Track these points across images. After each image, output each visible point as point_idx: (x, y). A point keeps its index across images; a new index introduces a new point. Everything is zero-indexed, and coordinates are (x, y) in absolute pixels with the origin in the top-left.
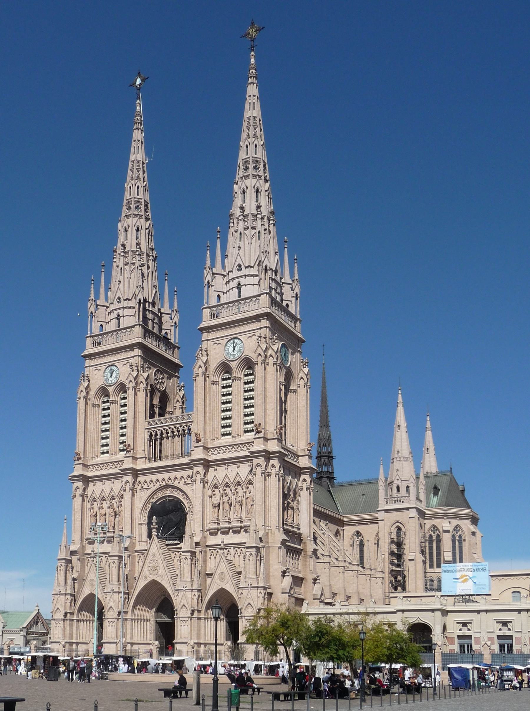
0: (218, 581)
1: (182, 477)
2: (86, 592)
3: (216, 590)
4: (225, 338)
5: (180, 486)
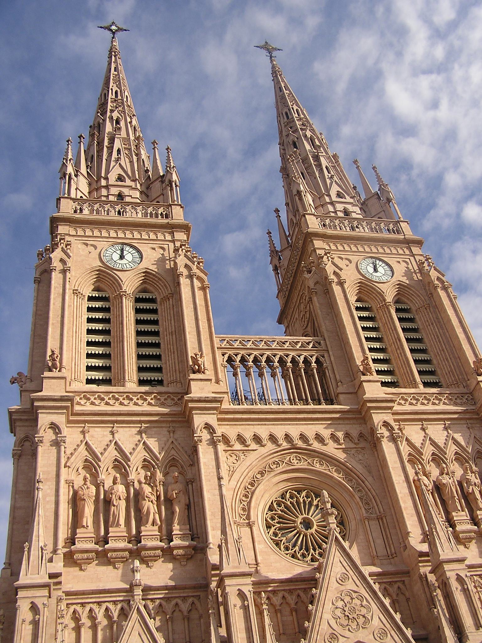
4: (355, 254)
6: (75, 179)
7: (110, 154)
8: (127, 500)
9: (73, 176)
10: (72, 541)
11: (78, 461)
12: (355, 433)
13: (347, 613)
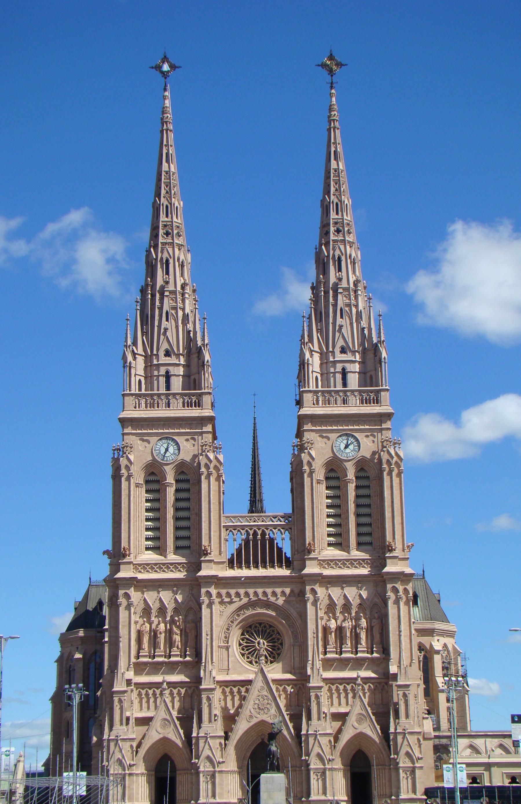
3: (353, 735)
6: (134, 362)
7: (161, 316)
8: (165, 632)
9: (132, 361)
10: (138, 657)
11: (140, 609)
12: (297, 591)
13: (260, 706)
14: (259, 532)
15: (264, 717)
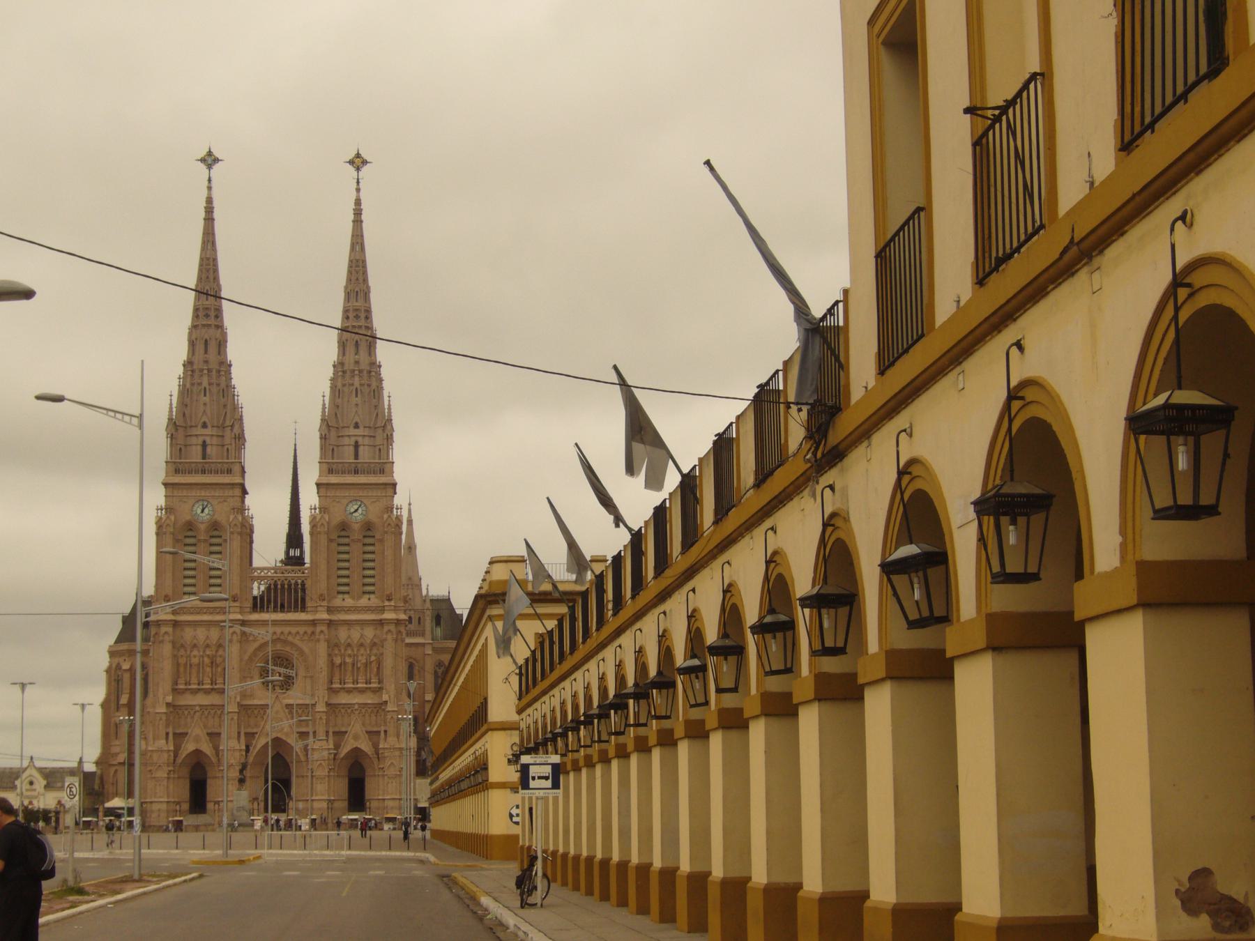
0: (352, 741)
1: (298, 633)
2: (189, 747)
5: (297, 641)
12: (309, 632)
14: (279, 583)
15: (279, 735)
